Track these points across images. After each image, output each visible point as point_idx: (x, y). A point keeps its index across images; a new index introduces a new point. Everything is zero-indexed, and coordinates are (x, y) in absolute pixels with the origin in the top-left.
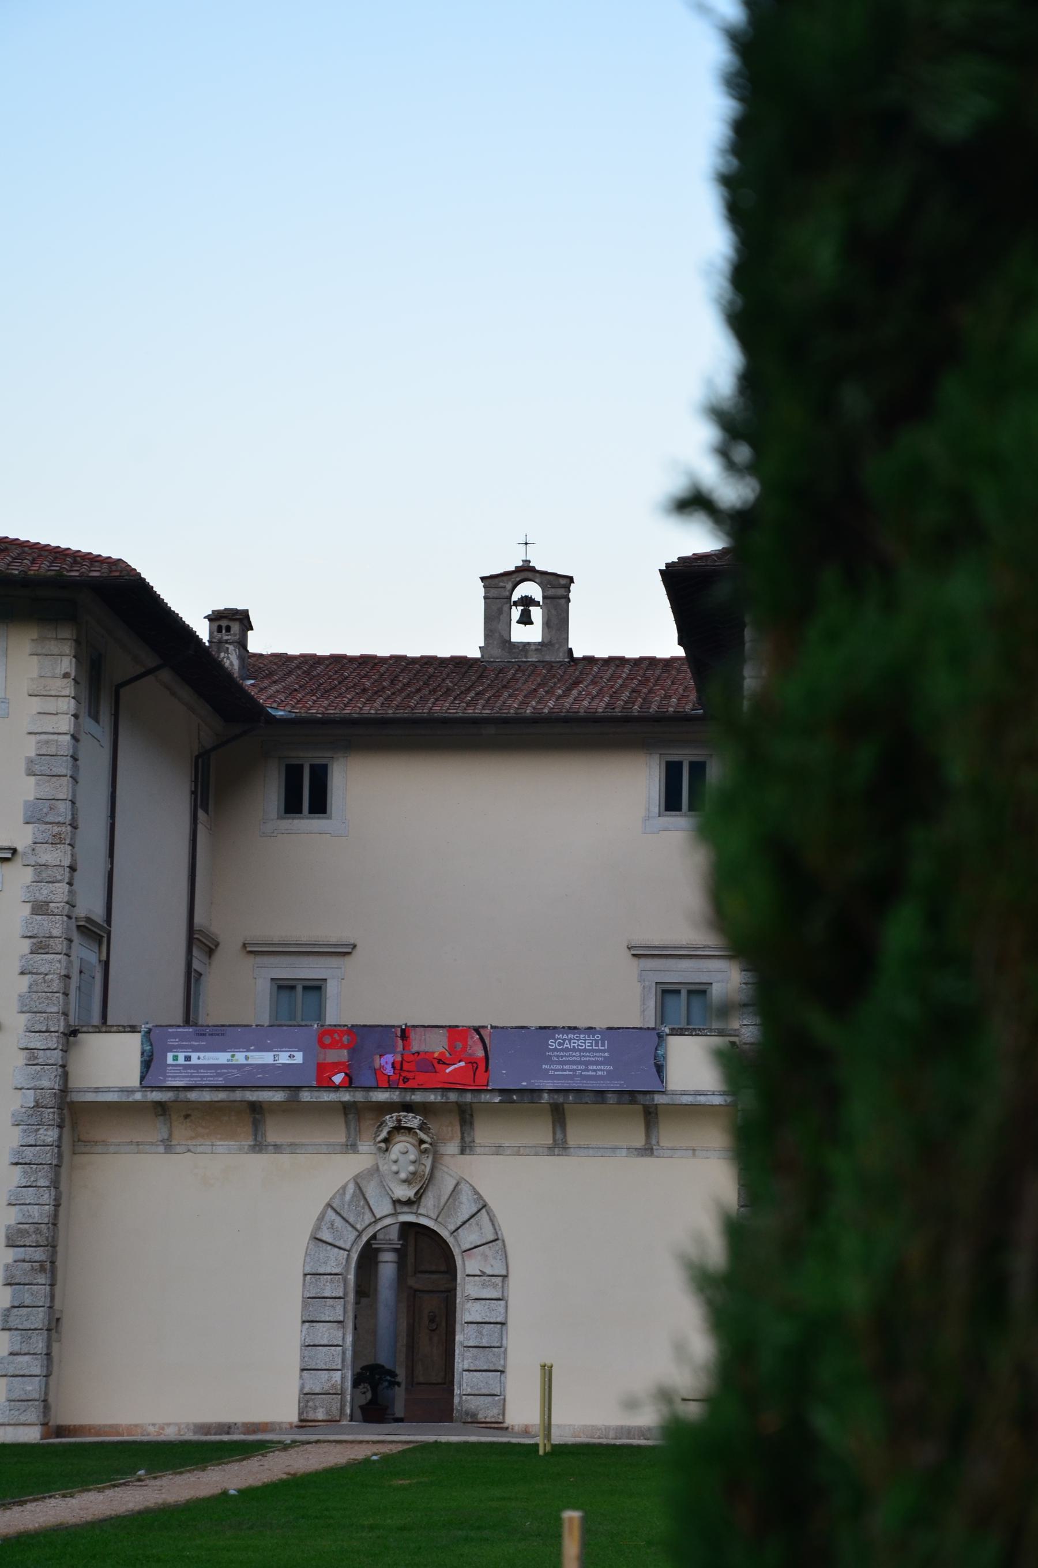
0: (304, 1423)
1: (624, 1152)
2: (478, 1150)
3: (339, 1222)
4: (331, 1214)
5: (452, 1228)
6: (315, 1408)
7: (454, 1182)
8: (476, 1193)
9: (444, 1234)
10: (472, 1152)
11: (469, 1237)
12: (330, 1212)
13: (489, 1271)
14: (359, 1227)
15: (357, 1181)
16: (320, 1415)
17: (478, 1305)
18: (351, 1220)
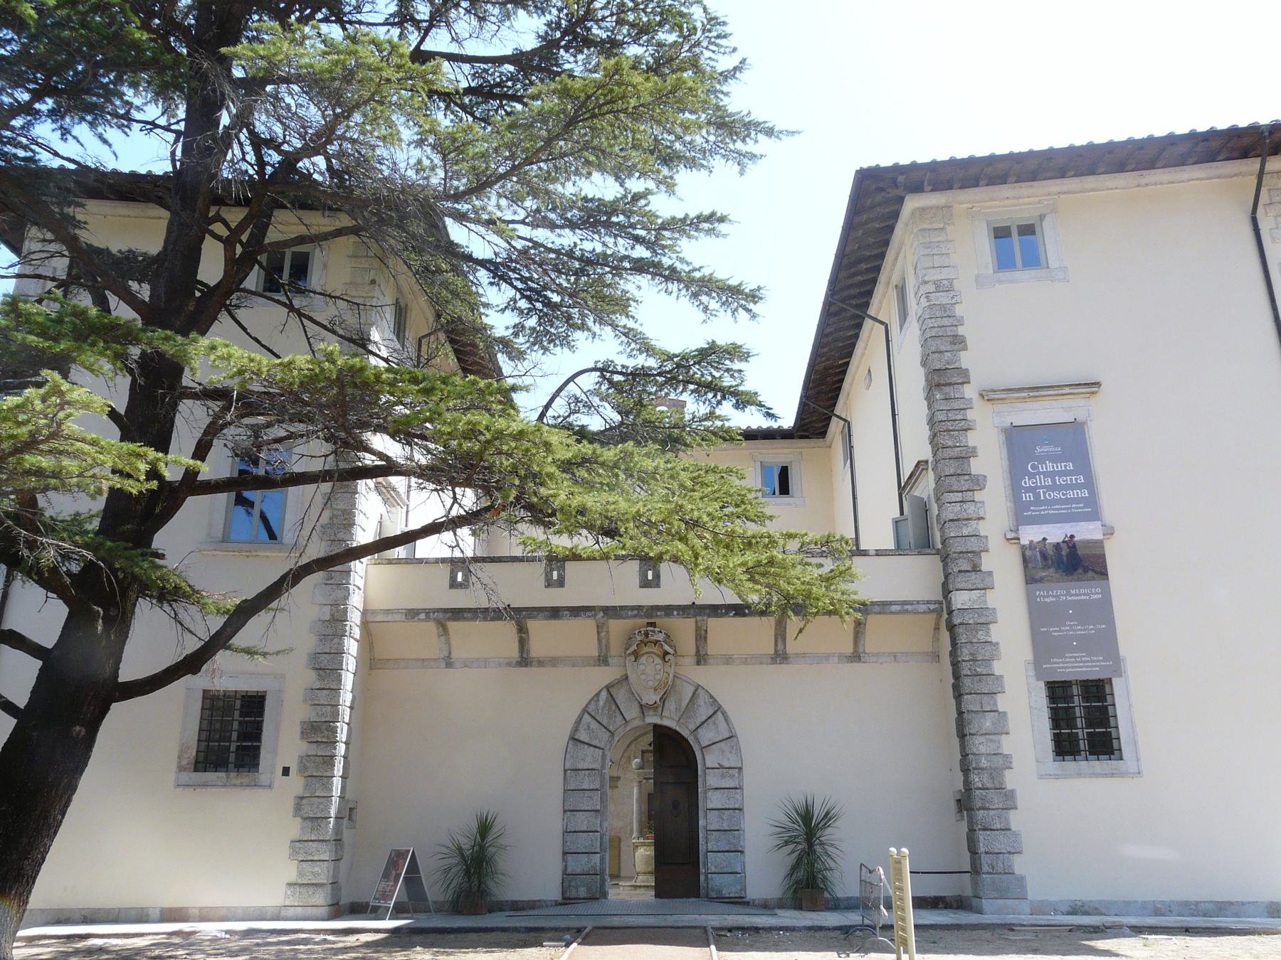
0: (567, 900)
1: (836, 660)
2: (711, 661)
3: (594, 725)
4: (587, 718)
5: (692, 727)
6: (577, 888)
7: (693, 689)
8: (712, 697)
9: (685, 733)
10: (706, 663)
11: (706, 736)
12: (586, 715)
13: (726, 764)
14: (611, 728)
15: (608, 688)
16: (583, 892)
17: (718, 794)
18: (605, 722)
